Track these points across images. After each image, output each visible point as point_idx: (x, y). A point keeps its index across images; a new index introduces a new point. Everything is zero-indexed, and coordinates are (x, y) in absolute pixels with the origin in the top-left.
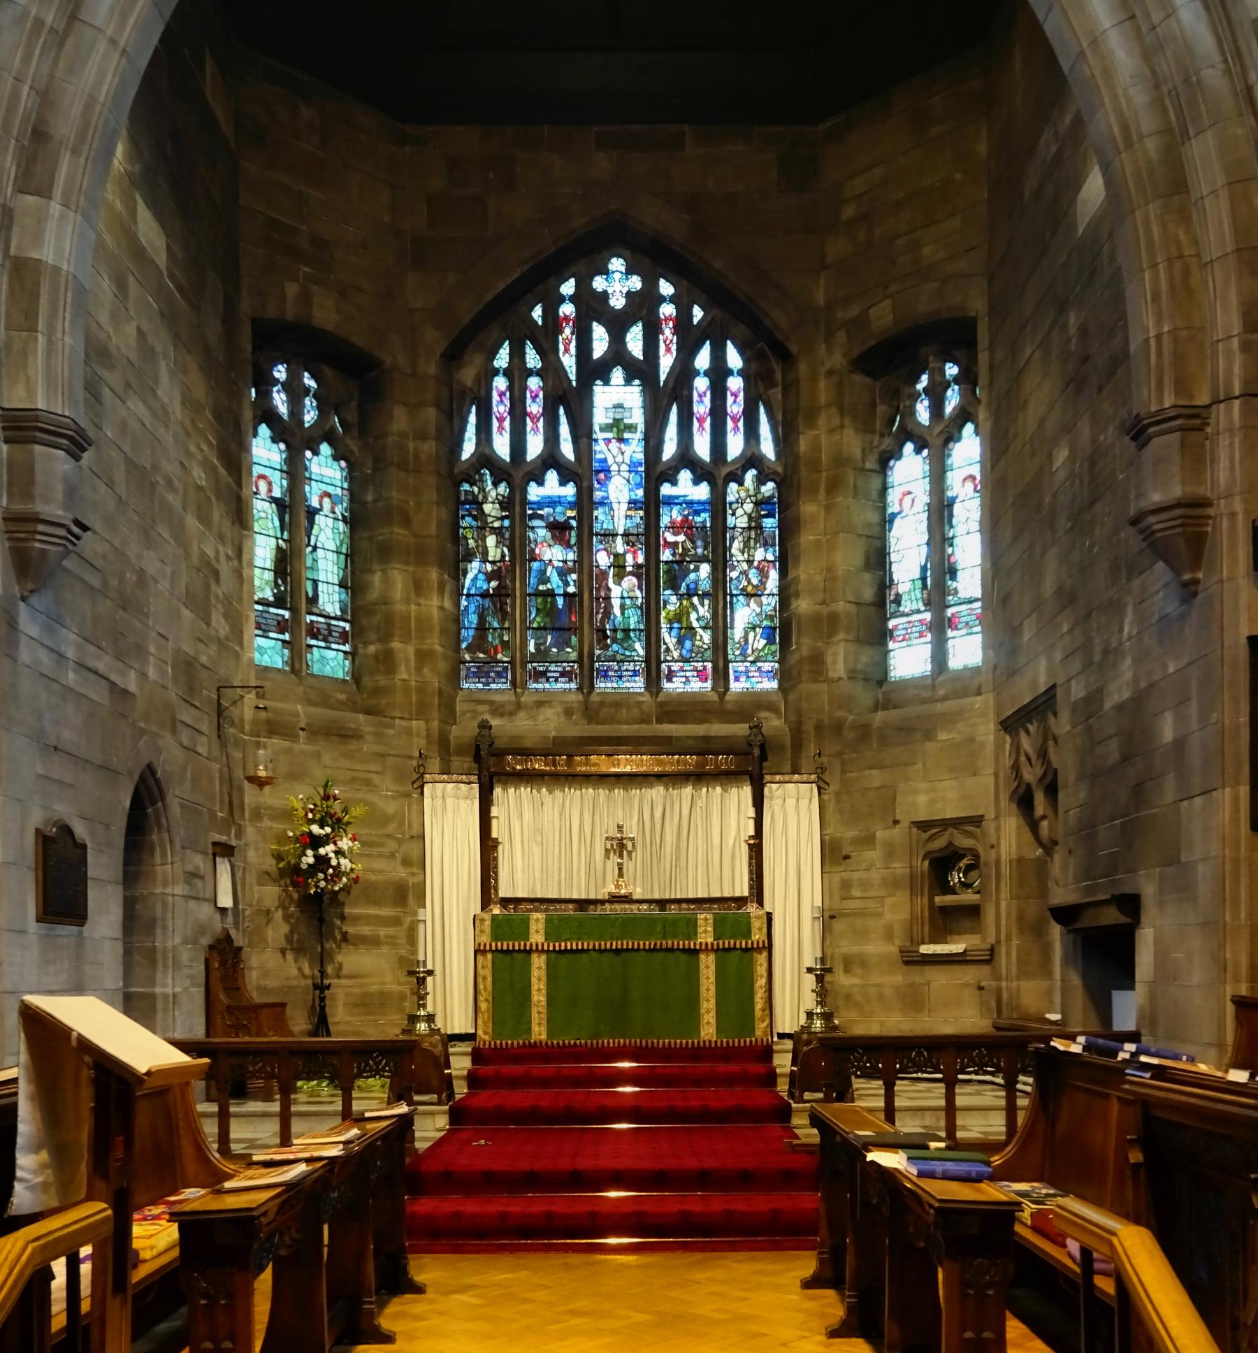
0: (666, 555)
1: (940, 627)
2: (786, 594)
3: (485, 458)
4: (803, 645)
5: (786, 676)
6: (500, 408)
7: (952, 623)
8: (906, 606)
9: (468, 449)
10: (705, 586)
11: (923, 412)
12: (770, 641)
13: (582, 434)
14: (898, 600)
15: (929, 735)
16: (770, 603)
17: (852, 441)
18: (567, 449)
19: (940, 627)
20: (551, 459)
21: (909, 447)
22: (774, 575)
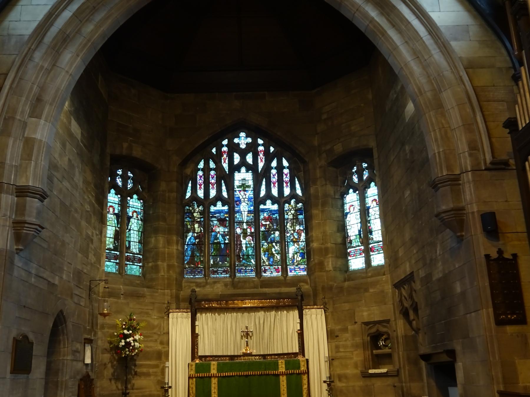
0: (263, 229)
1: (367, 252)
2: (308, 241)
3: (194, 197)
4: (315, 259)
5: (309, 270)
6: (200, 181)
7: (372, 250)
8: (354, 244)
9: (188, 195)
10: (278, 239)
11: (355, 179)
12: (303, 258)
13: (231, 189)
14: (351, 242)
15: (366, 290)
16: (302, 244)
17: (330, 189)
18: (225, 194)
19: (367, 252)
20: (219, 197)
21: (351, 191)
22: (303, 235)
